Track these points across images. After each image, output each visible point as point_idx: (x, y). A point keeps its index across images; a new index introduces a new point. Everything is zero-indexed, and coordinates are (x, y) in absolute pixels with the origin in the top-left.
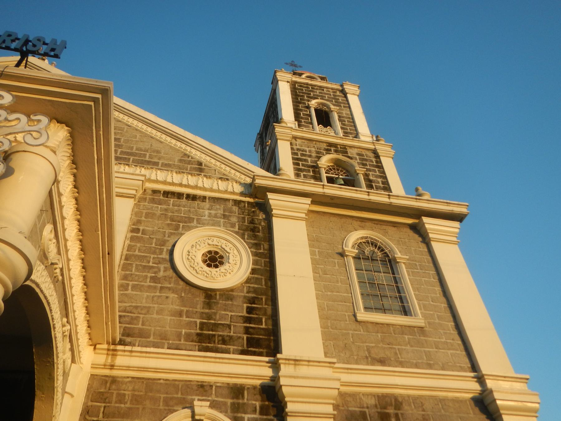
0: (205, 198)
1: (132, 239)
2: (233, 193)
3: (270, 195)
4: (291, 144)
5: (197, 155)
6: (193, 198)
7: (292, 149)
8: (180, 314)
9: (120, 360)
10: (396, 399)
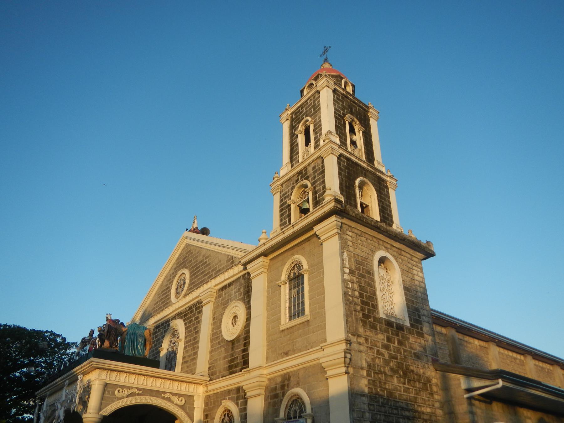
0: (233, 281)
1: (214, 324)
2: (241, 271)
3: (248, 266)
5: (232, 253)
6: (230, 285)
7: (280, 197)
8: (224, 358)
9: (210, 388)
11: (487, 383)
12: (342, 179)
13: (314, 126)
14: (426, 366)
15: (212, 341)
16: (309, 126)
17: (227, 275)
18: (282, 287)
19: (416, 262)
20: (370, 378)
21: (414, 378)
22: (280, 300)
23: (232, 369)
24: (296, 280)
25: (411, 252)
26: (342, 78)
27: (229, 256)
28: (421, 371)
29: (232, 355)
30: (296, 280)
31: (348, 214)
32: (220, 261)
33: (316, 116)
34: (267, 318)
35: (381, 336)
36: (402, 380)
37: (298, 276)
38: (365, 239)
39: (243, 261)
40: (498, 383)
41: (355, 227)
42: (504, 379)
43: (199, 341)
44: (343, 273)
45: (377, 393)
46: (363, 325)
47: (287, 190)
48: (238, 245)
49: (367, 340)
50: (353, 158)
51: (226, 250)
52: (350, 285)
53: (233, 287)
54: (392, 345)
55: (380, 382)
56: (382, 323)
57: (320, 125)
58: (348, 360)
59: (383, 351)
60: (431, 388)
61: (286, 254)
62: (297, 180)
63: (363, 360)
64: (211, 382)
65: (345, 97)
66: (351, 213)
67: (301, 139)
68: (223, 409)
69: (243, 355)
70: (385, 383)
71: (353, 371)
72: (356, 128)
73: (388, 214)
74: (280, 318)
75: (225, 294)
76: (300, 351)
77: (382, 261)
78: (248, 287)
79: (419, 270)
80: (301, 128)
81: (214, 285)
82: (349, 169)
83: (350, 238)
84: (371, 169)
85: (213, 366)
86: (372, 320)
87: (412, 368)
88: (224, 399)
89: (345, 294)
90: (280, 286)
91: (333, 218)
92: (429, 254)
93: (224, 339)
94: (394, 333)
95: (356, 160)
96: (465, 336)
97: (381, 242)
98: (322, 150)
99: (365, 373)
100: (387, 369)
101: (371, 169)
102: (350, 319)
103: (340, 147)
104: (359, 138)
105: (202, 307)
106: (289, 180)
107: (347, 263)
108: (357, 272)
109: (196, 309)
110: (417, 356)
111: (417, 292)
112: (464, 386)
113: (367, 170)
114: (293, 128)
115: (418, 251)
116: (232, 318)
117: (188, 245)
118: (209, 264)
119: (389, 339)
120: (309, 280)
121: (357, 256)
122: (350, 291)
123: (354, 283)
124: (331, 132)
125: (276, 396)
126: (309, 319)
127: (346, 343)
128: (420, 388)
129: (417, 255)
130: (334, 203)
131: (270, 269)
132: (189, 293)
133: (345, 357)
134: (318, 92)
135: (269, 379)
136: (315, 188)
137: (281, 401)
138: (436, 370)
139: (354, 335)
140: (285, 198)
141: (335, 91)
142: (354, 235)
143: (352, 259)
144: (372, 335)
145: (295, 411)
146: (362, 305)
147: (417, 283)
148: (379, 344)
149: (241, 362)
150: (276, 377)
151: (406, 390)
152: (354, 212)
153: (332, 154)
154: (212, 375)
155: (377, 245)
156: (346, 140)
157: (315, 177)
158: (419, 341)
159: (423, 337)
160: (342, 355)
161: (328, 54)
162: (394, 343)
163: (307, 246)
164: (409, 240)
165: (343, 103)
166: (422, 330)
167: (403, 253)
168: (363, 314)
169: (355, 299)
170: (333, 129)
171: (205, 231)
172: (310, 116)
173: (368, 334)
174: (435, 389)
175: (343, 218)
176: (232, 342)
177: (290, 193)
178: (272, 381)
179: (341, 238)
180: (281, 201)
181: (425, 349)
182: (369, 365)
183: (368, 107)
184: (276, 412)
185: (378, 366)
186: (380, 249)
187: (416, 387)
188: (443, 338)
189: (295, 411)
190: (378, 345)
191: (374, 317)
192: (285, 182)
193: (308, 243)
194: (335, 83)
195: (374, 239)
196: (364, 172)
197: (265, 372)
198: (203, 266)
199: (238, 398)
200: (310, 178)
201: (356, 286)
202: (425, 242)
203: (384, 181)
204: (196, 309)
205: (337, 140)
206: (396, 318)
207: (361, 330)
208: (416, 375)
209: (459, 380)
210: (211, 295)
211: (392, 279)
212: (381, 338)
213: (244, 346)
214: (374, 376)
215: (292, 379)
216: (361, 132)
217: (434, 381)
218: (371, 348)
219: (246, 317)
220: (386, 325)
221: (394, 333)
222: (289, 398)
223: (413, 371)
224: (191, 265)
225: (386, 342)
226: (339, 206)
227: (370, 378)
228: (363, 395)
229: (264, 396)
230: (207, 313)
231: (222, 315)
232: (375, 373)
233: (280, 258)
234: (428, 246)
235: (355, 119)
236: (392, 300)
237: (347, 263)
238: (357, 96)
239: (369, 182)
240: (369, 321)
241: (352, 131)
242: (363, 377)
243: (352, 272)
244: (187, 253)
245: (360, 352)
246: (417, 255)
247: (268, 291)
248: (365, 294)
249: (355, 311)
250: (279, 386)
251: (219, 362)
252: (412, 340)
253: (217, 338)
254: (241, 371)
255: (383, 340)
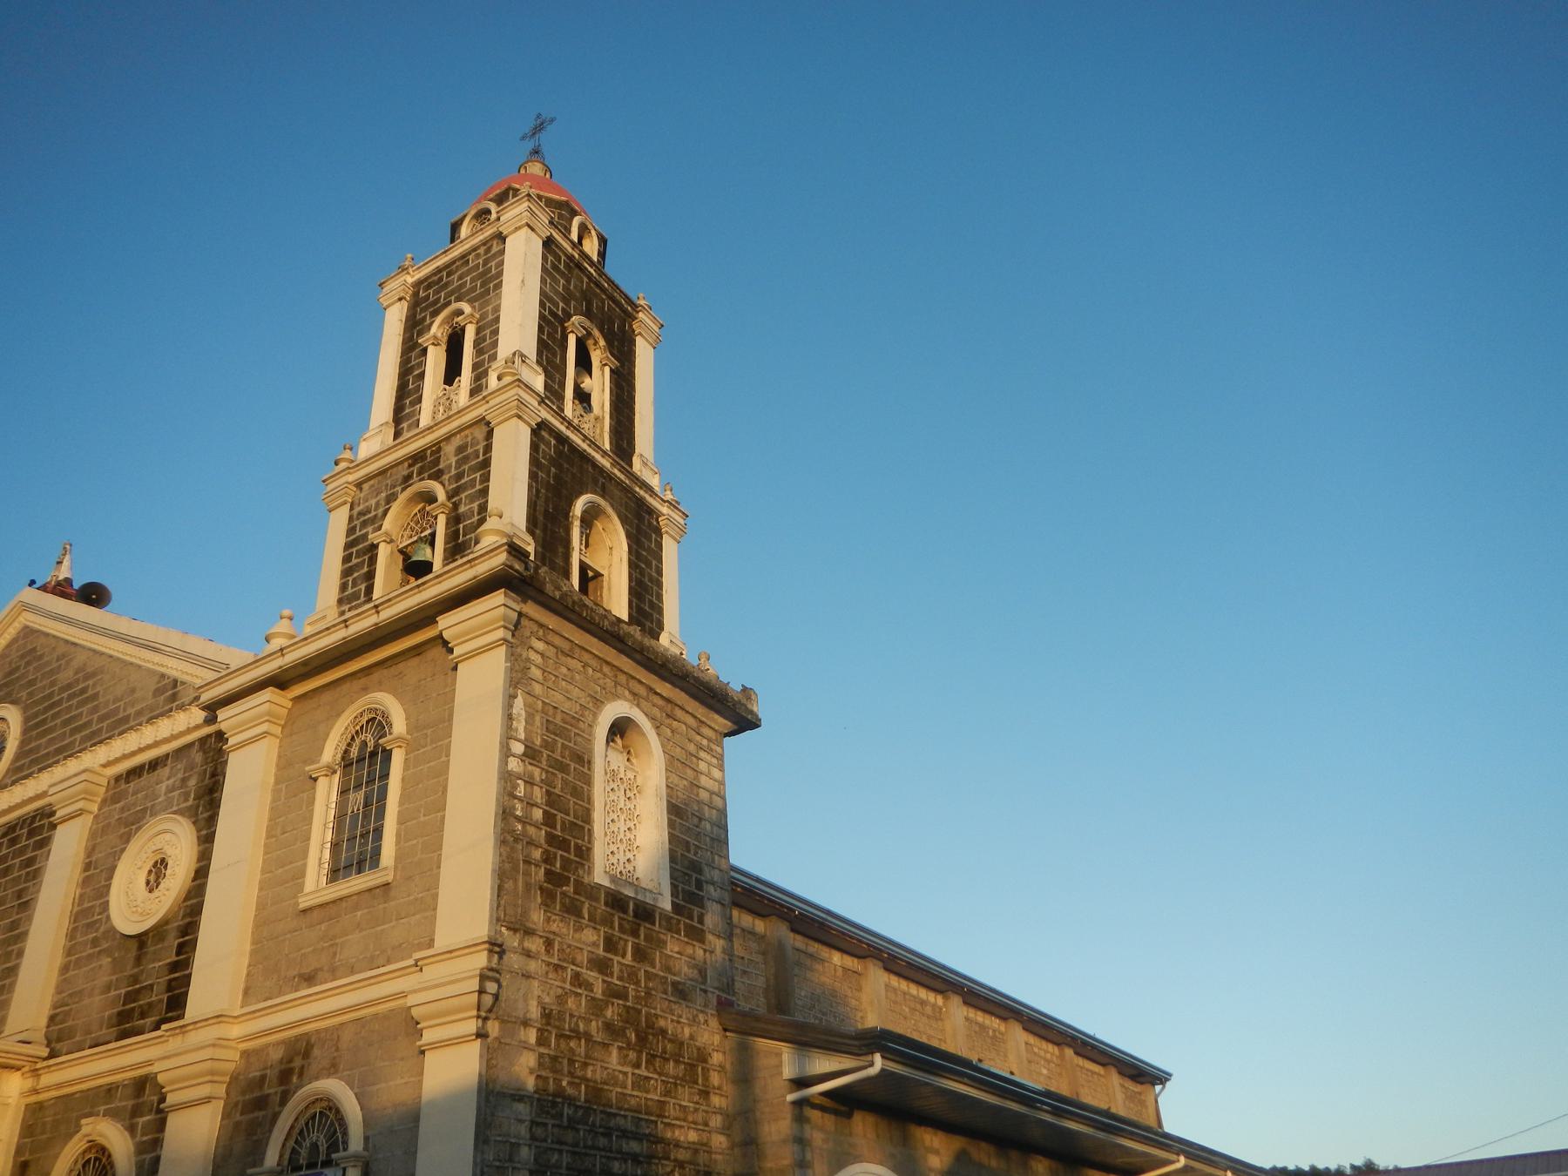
1: (86, 882)
2: (197, 727)
3: (222, 714)
4: (352, 508)
5: (175, 668)
6: (154, 765)
7: (351, 518)
8: (108, 988)
9: (47, 1079)
10: (308, 1043)
11: (846, 1062)
12: (538, 491)
13: (478, 332)
14: (701, 1017)
15: (71, 935)
16: (463, 330)
17: (148, 734)
18: (322, 783)
19: (709, 740)
20: (546, 1051)
21: (664, 1052)
22: (308, 819)
23: (127, 1023)
24: (366, 765)
25: (700, 711)
26: (574, 213)
27: (163, 676)
28: (687, 1031)
29: (135, 979)
30: (366, 765)
31: (542, 592)
32: (133, 691)
33: (487, 303)
34: (264, 871)
35: (589, 935)
36: (632, 1055)
37: (373, 754)
38: (579, 666)
39: (206, 697)
40: (872, 1064)
41: (557, 628)
42: (887, 1053)
43: (26, 933)
44: (506, 753)
45: (560, 1093)
46: (544, 904)
47: (373, 502)
48: (196, 645)
49: (549, 944)
50: (576, 439)
51: (157, 658)
52: (521, 790)
53: (164, 772)
54: (616, 959)
55: (571, 1062)
56: (597, 900)
57: (496, 332)
58: (488, 1000)
59: (591, 975)
60: (706, 1078)
61: (346, 687)
62: (408, 478)
63: (531, 999)
64: (52, 1062)
65: (575, 265)
66: (549, 588)
67: (435, 361)
68: (83, 1145)
69: (170, 981)
70: (585, 1065)
71: (501, 1029)
72: (596, 356)
73: (652, 605)
74: (302, 874)
75: (135, 793)
76: (352, 971)
77: (620, 729)
78: (213, 775)
79: (714, 761)
80: (438, 328)
81: (103, 761)
82: (559, 467)
83: (538, 659)
84: (622, 477)
85: (67, 1013)
86: (570, 889)
87: (662, 1023)
88: (90, 1115)
89: (505, 814)
90: (315, 780)
91: (498, 597)
92: (744, 721)
93: (113, 930)
94: (627, 926)
95: (584, 446)
96: (811, 942)
97: (622, 678)
98: (492, 403)
99: (532, 1036)
100: (594, 1027)
101: (622, 477)
102: (509, 885)
103: (542, 402)
104: (599, 385)
105: (53, 826)
106: (382, 472)
107: (520, 727)
108: (545, 753)
109: (31, 834)
110: (681, 992)
111: (700, 819)
112: (788, 1072)
113: (610, 477)
114: (414, 327)
115: (718, 712)
116: (149, 865)
117: (28, 632)
118: (95, 696)
119: (610, 945)
120: (406, 768)
121: (551, 711)
122: (518, 805)
123: (532, 784)
124: (522, 355)
125: (261, 1103)
126: (390, 878)
127: (490, 951)
128: (676, 1078)
129: (714, 720)
130: (501, 558)
131: (289, 725)
132: (13, 783)
133: (481, 992)
134: (501, 238)
135: (246, 1054)
136: (456, 506)
137: (275, 1117)
138: (725, 1030)
139: (515, 931)
140: (364, 524)
141: (548, 243)
142: (551, 652)
143: (538, 718)
144: (564, 930)
145: (315, 1146)
146: (548, 847)
147: (704, 795)
148: (583, 958)
149: (161, 1001)
150: (267, 1046)
151: (640, 1083)
152: (558, 588)
153: (519, 417)
154: (59, 1040)
155: (609, 683)
156: (562, 385)
157: (459, 476)
158: (689, 950)
159: (702, 941)
160: (474, 984)
161: (544, 137)
162: (624, 956)
163: (411, 667)
164: (697, 679)
165: (568, 281)
166: (701, 921)
167: (679, 713)
168: (548, 873)
169: (531, 830)
170: (531, 351)
171: (94, 595)
172: (470, 302)
173: (554, 927)
174: (715, 1079)
175: (524, 602)
176: (141, 939)
177: (381, 510)
178: (252, 1060)
179: (513, 656)
180: (351, 531)
181: (702, 972)
182: (547, 1015)
183: (635, 306)
184: (255, 1152)
185: (571, 1016)
186: (616, 696)
187: (667, 1075)
188: (754, 946)
189: (315, 1146)
190: (579, 958)
191: (579, 884)
192: (369, 478)
193: (414, 662)
194: (551, 223)
195: (606, 669)
196: (601, 481)
197: (236, 1031)
198: (74, 701)
199: (136, 1112)
200: (446, 477)
201: (538, 794)
202: (739, 688)
203: (651, 511)
204: (31, 834)
205: (538, 382)
206: (637, 888)
207: (537, 917)
208: (671, 1041)
209: (779, 1055)
210: (86, 791)
211: (639, 782)
212: (590, 938)
213: (178, 954)
214: (558, 1045)
215: (316, 1052)
216: (607, 369)
217: (717, 1058)
218: (557, 967)
219: (194, 866)
220: (606, 904)
221: (627, 926)
222: (300, 1108)
223: (663, 1032)
224: (31, 695)
225: (601, 951)
226: (517, 567)
227: (546, 1051)
228: (519, 1096)
229: (222, 1103)
230: (67, 847)
231: (116, 855)
232: (560, 1036)
233: (327, 697)
234: (744, 701)
235: (596, 333)
236: (631, 838)
237: (520, 727)
238: (608, 270)
239: (610, 510)
240: (564, 894)
241: (584, 363)
242: (525, 1046)
243: (531, 754)
244: (22, 657)
245: (527, 976)
246: (714, 720)
247: (276, 792)
248: (560, 815)
249: (527, 862)
250: (272, 1074)
251: (86, 1001)
252: (672, 947)
253: (89, 926)
254: (157, 1028)
255: (594, 944)
